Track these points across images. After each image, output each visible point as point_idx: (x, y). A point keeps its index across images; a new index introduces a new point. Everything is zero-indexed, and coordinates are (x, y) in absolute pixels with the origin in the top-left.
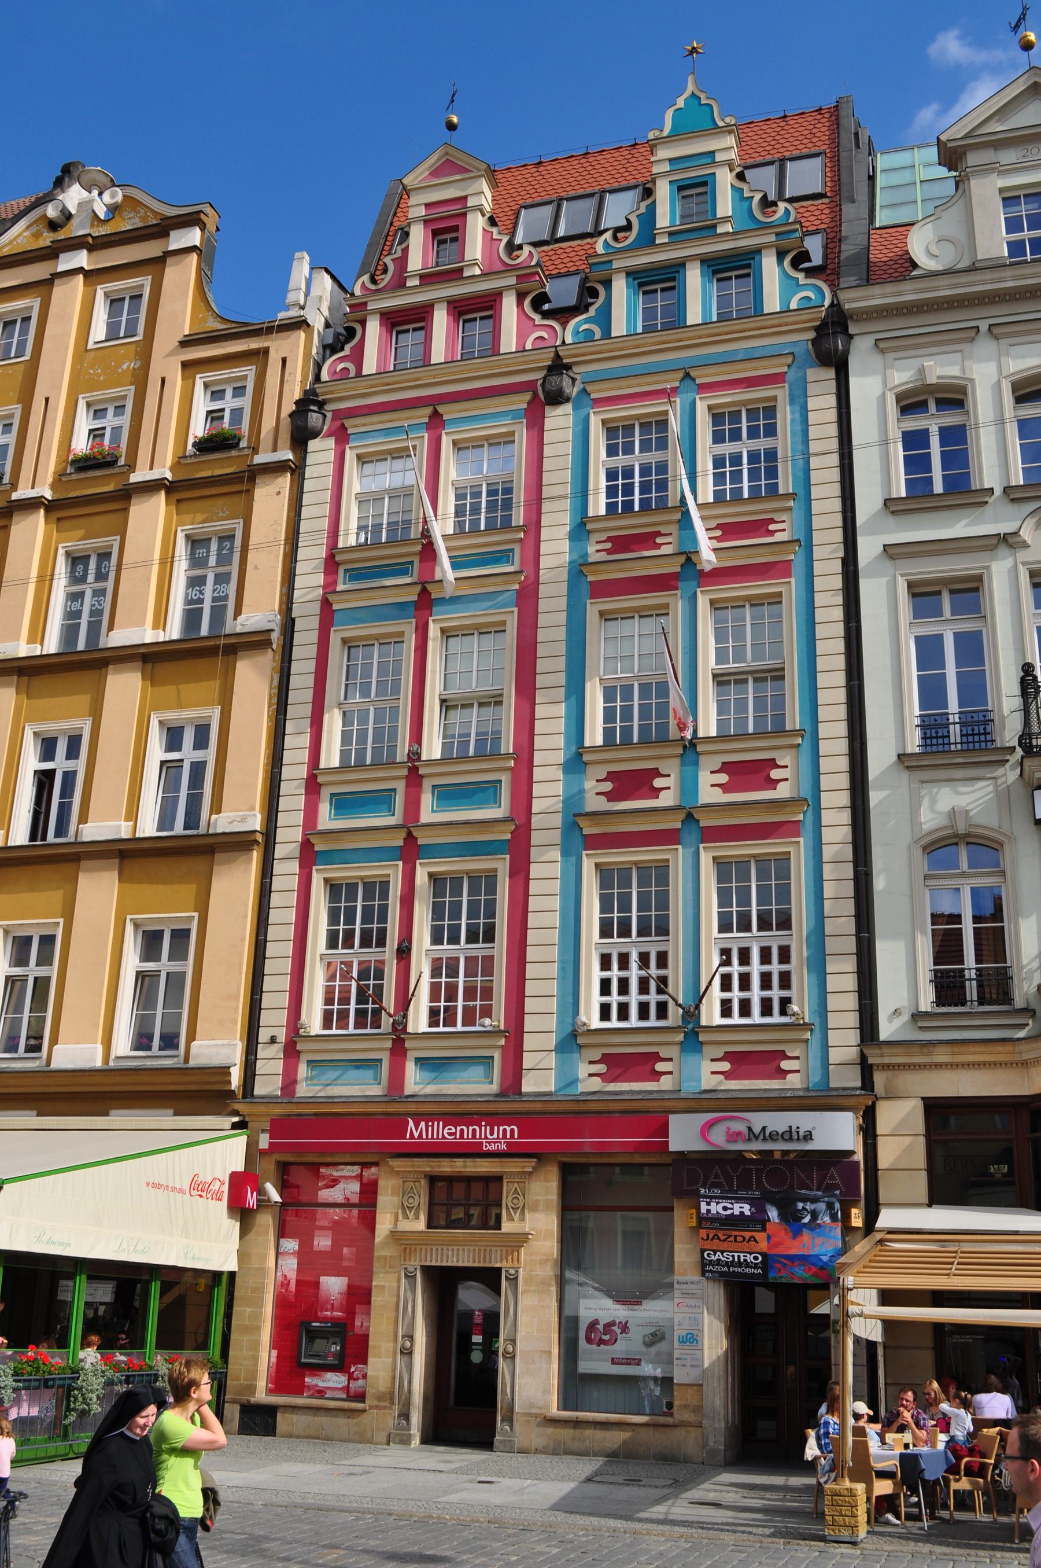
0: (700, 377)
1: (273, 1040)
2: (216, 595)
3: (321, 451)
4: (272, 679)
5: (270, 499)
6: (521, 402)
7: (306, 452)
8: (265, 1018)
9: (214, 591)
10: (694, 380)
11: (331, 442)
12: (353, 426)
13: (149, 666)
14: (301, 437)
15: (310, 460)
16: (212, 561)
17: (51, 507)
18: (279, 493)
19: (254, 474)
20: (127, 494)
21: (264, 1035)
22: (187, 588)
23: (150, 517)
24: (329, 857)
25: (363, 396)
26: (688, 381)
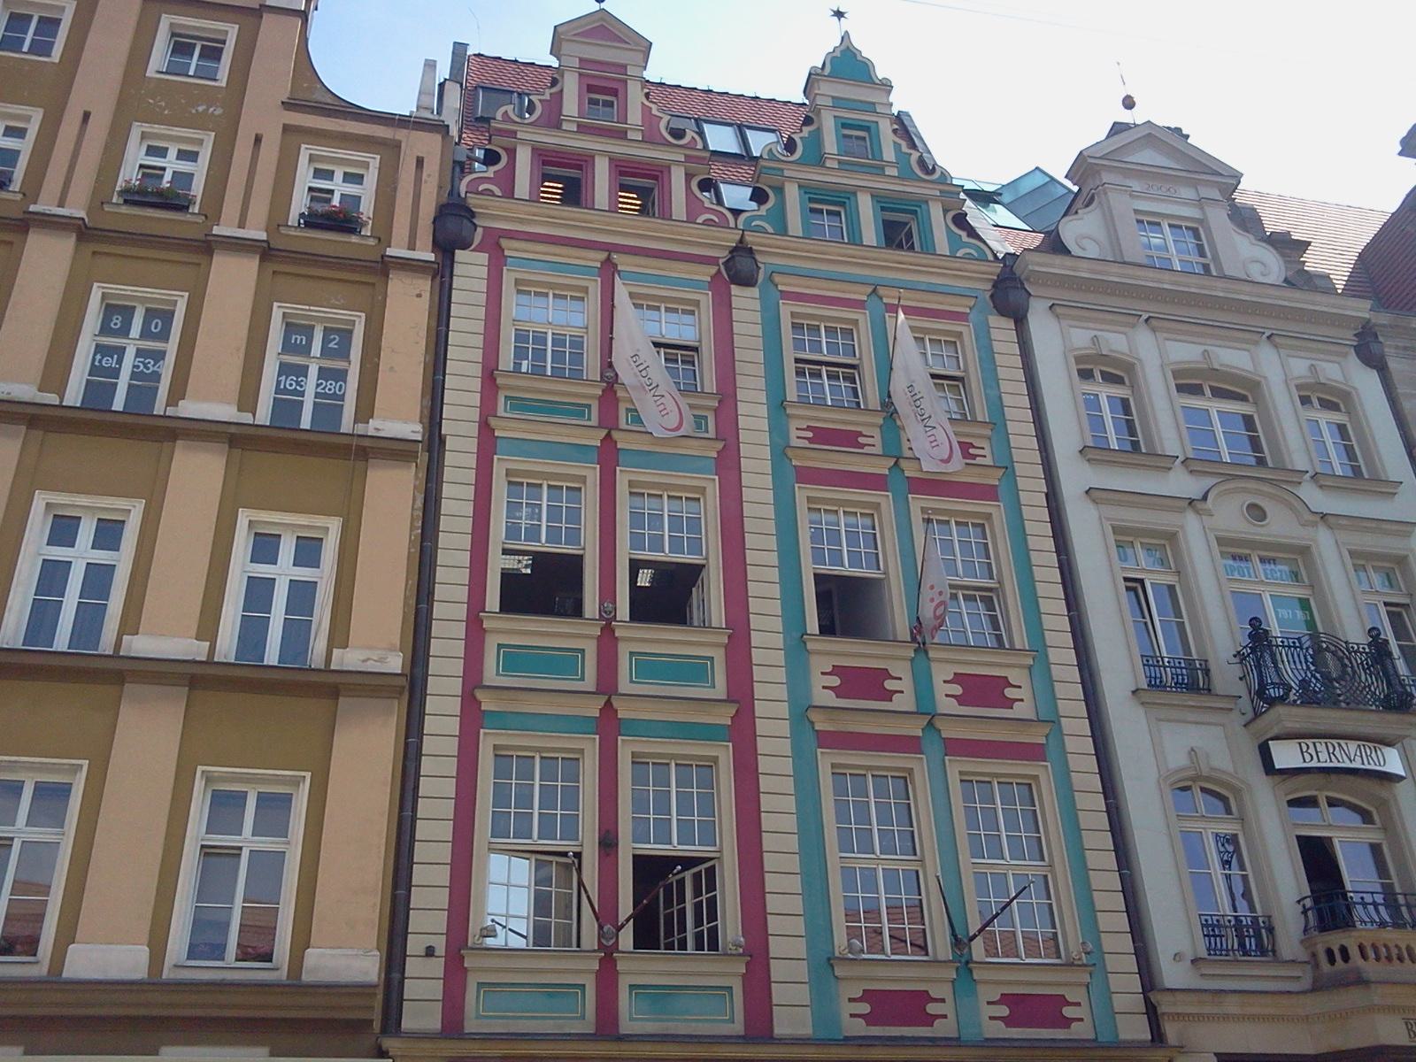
0: (888, 297)
1: (430, 952)
2: (319, 390)
3: (471, 267)
4: (414, 500)
5: (407, 302)
6: (705, 273)
7: (453, 261)
8: (416, 921)
9: (318, 385)
10: (881, 298)
11: (483, 258)
12: (510, 248)
13: (237, 452)
14: (447, 246)
15: (457, 270)
16: (316, 349)
17: (84, 232)
18: (419, 296)
19: (385, 267)
20: (207, 246)
21: (415, 945)
22: (279, 375)
23: (233, 279)
24: (502, 720)
25: (521, 221)
26: (874, 298)
